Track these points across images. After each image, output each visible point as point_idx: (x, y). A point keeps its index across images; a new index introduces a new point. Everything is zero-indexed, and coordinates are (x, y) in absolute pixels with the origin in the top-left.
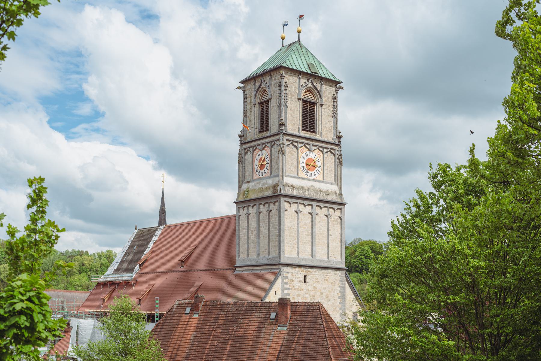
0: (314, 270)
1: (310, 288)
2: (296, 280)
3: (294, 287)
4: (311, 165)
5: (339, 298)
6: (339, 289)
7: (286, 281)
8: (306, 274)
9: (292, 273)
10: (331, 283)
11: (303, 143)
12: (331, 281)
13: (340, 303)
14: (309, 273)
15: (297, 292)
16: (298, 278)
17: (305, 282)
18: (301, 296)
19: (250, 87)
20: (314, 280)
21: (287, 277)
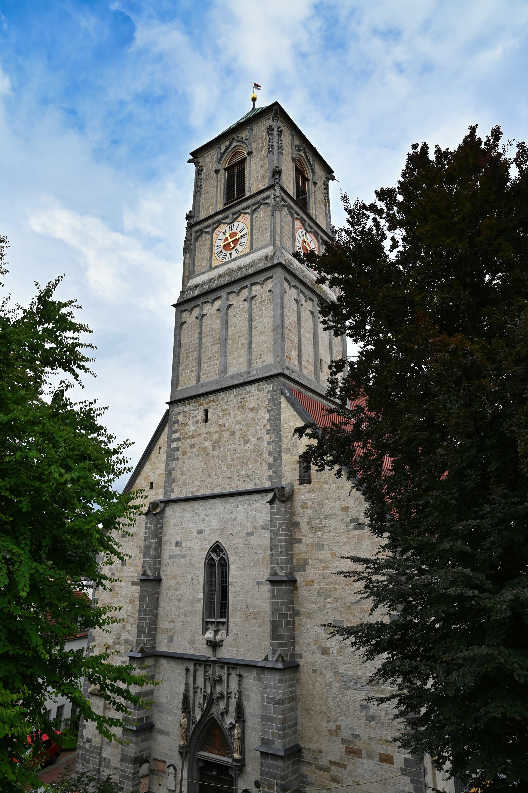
0: (221, 395)
2: (190, 423)
3: (186, 433)
6: (267, 416)
7: (175, 427)
8: (205, 407)
10: (252, 410)
12: (252, 406)
13: (269, 443)
15: (190, 442)
16: (193, 417)
18: (197, 447)
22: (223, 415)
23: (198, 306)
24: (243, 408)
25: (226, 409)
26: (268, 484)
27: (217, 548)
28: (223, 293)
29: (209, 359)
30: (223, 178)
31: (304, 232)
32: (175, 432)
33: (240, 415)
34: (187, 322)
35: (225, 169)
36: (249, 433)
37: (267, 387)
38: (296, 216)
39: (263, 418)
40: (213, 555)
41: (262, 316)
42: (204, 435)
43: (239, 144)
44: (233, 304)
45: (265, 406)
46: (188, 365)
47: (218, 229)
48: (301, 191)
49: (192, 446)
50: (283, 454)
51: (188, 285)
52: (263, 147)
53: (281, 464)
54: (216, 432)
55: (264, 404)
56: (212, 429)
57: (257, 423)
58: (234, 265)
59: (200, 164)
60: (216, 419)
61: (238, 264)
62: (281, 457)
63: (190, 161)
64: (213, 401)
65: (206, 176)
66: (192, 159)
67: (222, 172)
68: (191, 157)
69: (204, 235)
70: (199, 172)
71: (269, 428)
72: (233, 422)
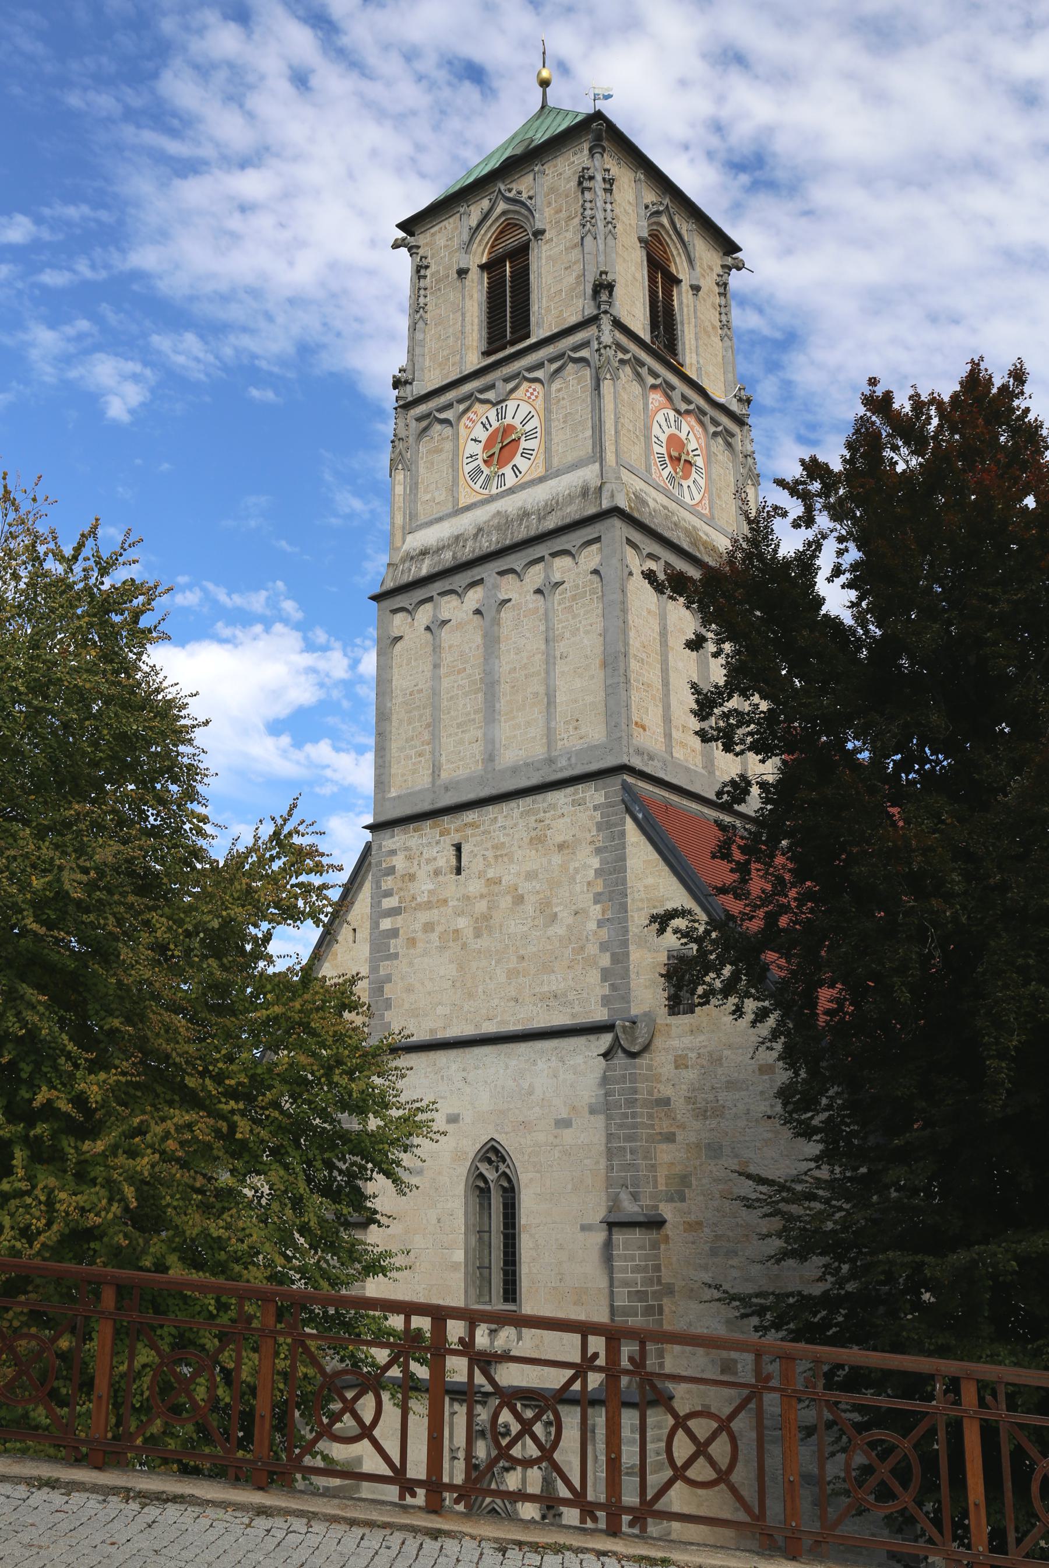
0: (491, 810)
2: (421, 874)
3: (414, 898)
4: (503, 446)
5: (597, 899)
6: (595, 862)
7: (388, 883)
8: (456, 838)
9: (407, 849)
10: (561, 847)
12: (560, 839)
13: (600, 924)
14: (469, 832)
15: (423, 917)
16: (428, 861)
18: (439, 929)
20: (490, 854)
21: (391, 871)
22: (496, 857)
23: (430, 599)
24: (541, 842)
25: (503, 843)
26: (599, 1015)
27: (493, 1153)
28: (488, 572)
29: (459, 725)
30: (477, 286)
31: (672, 414)
32: (388, 894)
34: (406, 638)
35: (482, 267)
36: (555, 901)
37: (593, 794)
38: (651, 381)
39: (586, 866)
40: (484, 1168)
41: (578, 629)
42: (456, 903)
43: (512, 207)
44: (510, 600)
45: (589, 839)
46: (412, 739)
47: (470, 414)
48: (663, 318)
49: (429, 927)
50: (632, 948)
51: (405, 547)
52: (570, 218)
53: (627, 969)
54: (482, 896)
55: (588, 836)
56: (471, 889)
57: (574, 879)
58: (510, 505)
59: (421, 252)
60: (481, 867)
61: (520, 504)
62: (627, 954)
63: (396, 246)
64: (472, 825)
65: (438, 282)
66: (404, 239)
67: (474, 274)
68: (401, 234)
69: (437, 427)
70: (420, 270)
71: (599, 889)
72: (518, 874)
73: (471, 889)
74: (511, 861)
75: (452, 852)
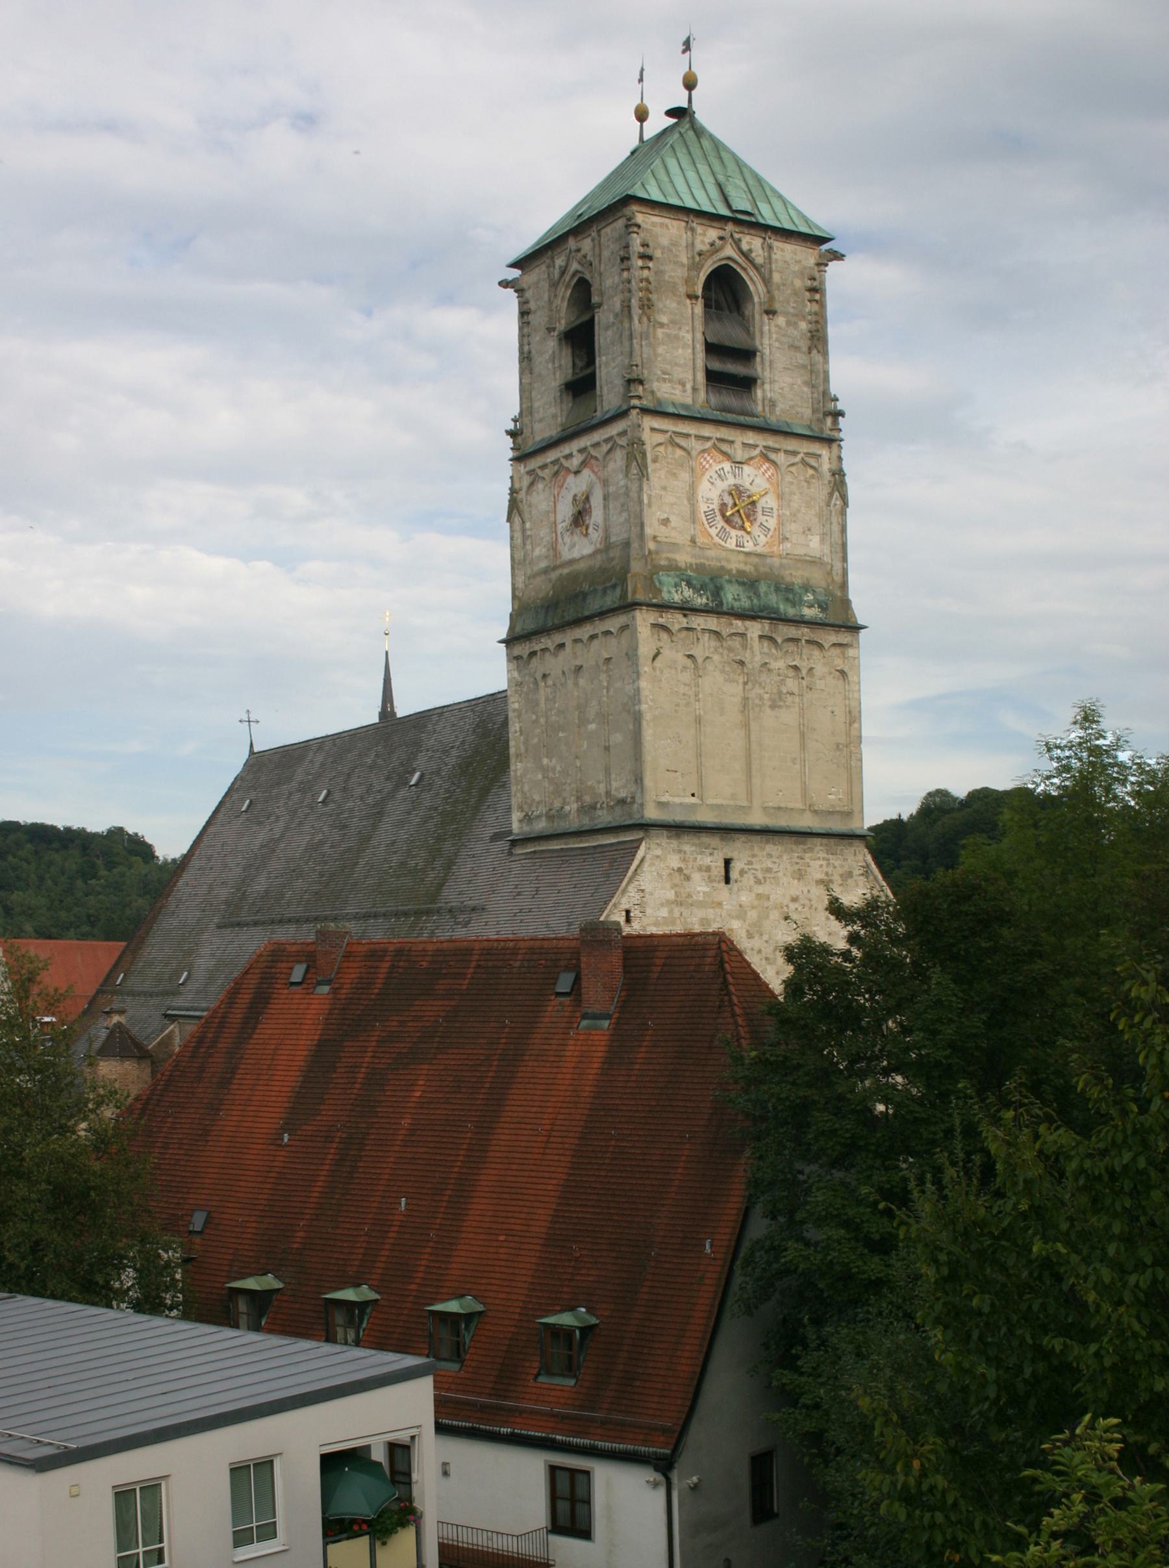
1: (745, 898)
2: (696, 876)
3: (689, 896)
11: (708, 439)
17: (727, 880)
19: (538, 274)
33: (796, 888)
73: (744, 899)
74: (778, 884)
75: (721, 864)
